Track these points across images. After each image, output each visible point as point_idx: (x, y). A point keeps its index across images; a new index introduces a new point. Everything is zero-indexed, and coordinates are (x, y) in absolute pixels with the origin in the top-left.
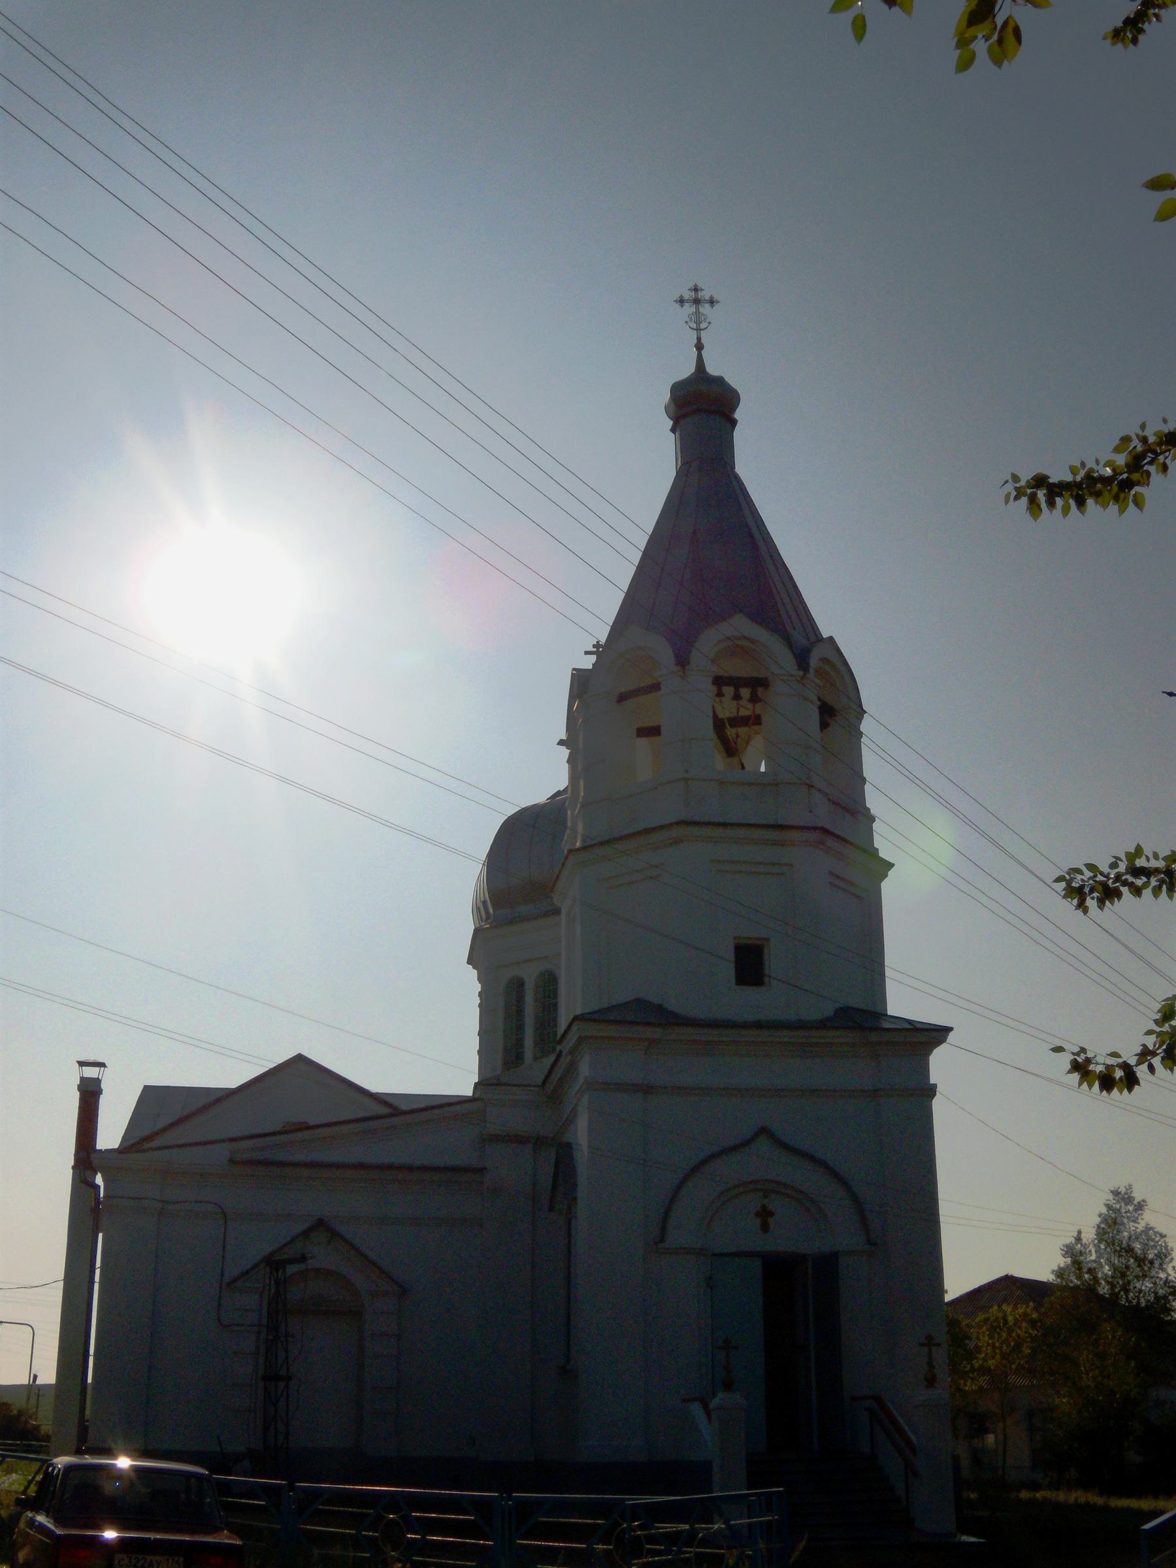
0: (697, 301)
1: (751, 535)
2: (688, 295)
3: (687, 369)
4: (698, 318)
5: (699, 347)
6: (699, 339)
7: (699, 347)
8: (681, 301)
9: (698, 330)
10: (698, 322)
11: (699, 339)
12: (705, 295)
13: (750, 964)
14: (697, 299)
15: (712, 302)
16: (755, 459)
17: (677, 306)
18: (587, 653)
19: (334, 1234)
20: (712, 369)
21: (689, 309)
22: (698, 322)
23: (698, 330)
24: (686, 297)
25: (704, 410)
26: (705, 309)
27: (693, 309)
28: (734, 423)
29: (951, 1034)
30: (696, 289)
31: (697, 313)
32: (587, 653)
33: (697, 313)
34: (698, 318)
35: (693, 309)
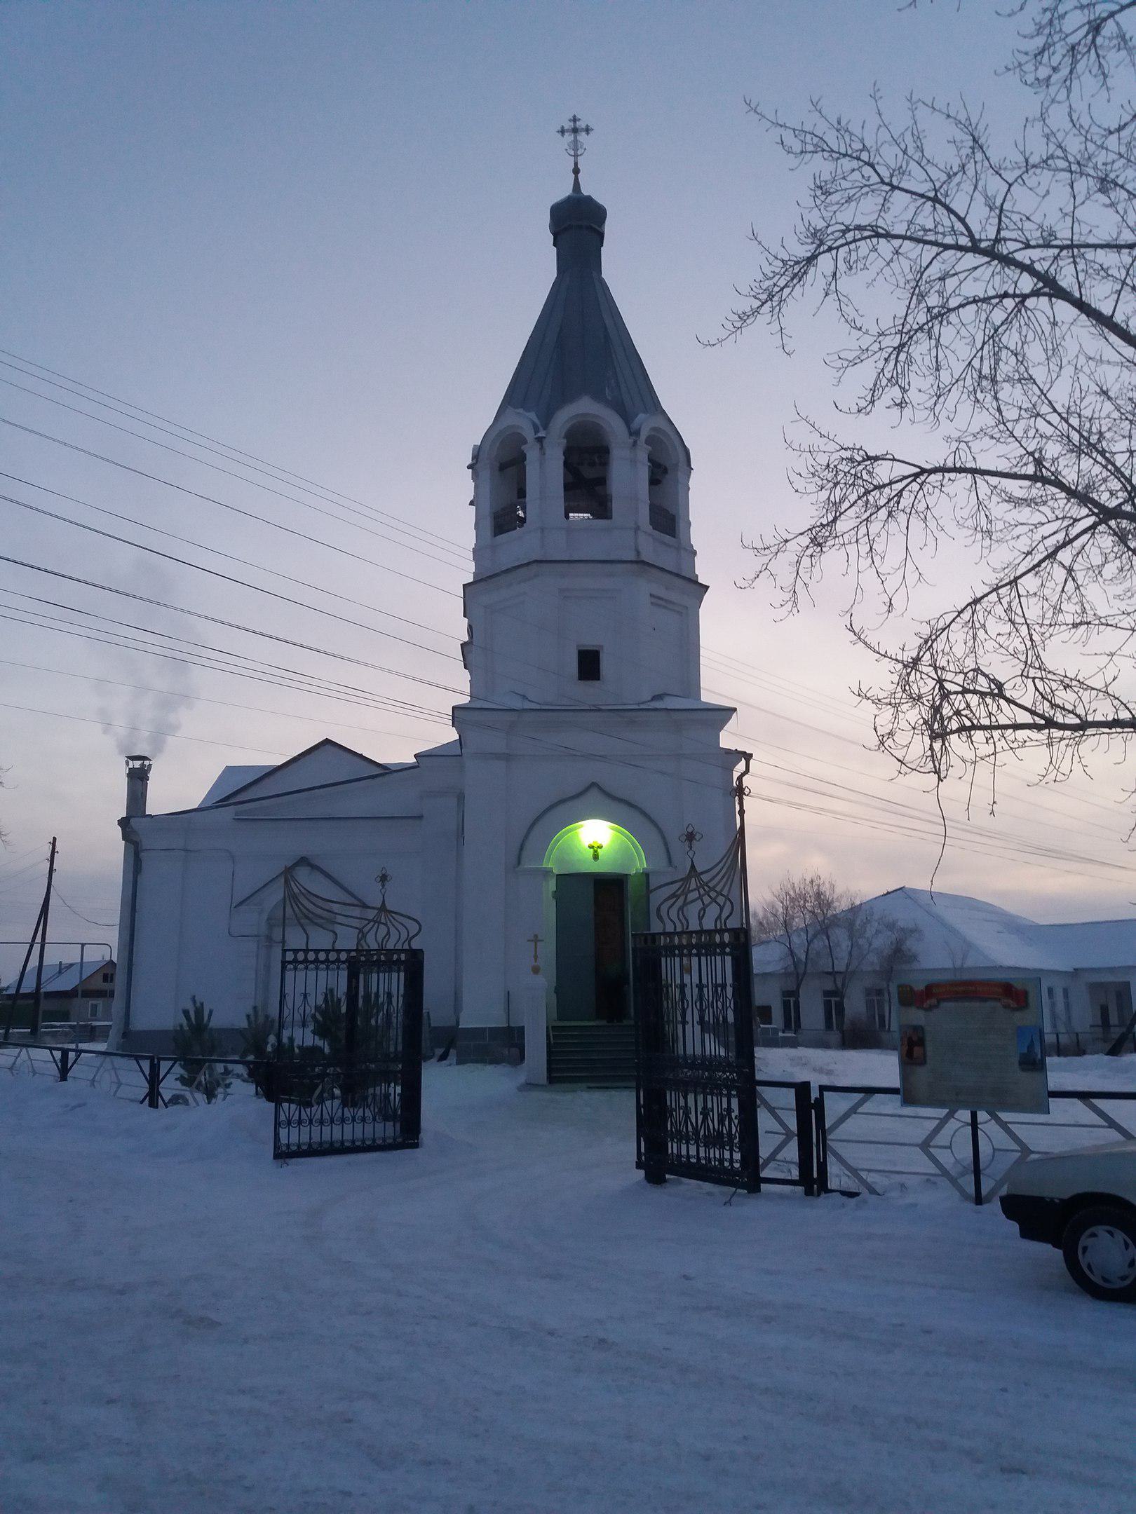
0: (575, 131)
1: (607, 337)
2: (568, 125)
3: (565, 191)
4: (576, 145)
5: (576, 171)
6: (576, 164)
7: (576, 171)
8: (563, 132)
9: (576, 156)
10: (576, 149)
11: (576, 164)
12: (581, 125)
13: (589, 665)
14: (575, 129)
15: (588, 130)
16: (619, 268)
17: (559, 135)
18: (193, 999)
19: (314, 867)
20: (586, 191)
21: (569, 137)
22: (576, 149)
23: (576, 156)
24: (566, 127)
25: (578, 226)
26: (582, 137)
27: (572, 138)
28: (602, 236)
29: (731, 725)
30: (575, 120)
31: (575, 141)
32: (193, 999)
33: (575, 141)
34: (576, 145)
35: (572, 138)
